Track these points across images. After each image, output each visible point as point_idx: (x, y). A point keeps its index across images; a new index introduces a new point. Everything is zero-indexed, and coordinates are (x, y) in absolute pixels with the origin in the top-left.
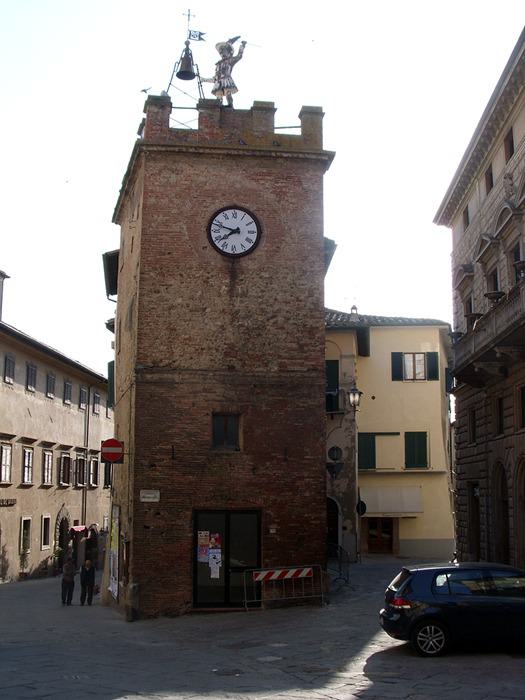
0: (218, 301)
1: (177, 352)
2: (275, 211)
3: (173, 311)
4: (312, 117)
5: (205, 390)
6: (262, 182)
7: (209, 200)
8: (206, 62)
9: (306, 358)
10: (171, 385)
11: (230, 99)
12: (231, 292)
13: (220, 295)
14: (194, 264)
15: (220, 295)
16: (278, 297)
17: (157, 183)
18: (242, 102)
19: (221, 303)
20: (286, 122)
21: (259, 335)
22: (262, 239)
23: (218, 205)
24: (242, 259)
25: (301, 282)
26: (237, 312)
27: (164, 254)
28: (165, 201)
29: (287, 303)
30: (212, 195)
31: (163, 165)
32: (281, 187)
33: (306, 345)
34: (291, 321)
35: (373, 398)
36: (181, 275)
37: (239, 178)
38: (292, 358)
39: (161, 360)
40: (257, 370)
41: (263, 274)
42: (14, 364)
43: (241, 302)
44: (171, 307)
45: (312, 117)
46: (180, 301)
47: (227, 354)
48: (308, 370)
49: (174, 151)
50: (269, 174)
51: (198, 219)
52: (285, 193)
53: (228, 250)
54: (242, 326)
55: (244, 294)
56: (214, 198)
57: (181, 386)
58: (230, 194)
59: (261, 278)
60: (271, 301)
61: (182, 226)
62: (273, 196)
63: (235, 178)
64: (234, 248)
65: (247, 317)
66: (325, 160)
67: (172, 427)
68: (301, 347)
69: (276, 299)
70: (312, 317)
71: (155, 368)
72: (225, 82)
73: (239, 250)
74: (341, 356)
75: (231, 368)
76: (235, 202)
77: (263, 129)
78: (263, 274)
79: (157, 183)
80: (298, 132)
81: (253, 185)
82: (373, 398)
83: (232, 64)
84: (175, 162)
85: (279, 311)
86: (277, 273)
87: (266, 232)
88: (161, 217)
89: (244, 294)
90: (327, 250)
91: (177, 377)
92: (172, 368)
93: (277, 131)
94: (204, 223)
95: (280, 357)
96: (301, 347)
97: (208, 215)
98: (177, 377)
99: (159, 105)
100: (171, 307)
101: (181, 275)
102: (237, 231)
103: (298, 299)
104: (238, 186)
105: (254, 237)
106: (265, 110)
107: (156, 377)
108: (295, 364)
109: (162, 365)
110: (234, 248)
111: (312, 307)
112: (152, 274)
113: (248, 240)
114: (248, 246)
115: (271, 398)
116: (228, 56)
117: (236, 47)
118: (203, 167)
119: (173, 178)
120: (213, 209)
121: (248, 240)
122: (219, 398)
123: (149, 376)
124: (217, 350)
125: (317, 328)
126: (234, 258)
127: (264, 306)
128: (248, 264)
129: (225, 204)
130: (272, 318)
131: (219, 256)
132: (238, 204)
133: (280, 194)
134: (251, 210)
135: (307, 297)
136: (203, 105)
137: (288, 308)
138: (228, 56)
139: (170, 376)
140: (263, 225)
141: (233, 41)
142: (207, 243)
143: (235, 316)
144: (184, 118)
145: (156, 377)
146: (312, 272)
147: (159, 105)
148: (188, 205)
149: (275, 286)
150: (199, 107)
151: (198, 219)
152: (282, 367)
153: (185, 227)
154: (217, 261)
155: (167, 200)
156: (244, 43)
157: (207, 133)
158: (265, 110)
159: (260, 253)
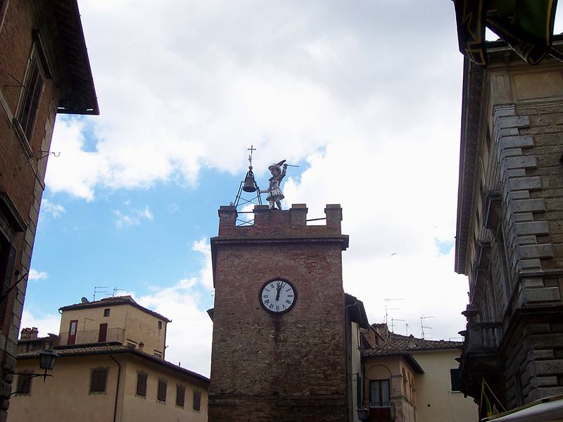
0: (266, 345)
1: (238, 382)
2: (307, 280)
3: (235, 354)
4: (334, 212)
5: (257, 410)
7: (261, 275)
8: (262, 176)
9: (331, 385)
10: (234, 407)
11: (279, 204)
12: (276, 339)
14: (251, 320)
18: (286, 205)
19: (269, 347)
20: (316, 216)
21: (296, 369)
23: (268, 278)
25: (327, 330)
26: (281, 353)
27: (229, 314)
29: (315, 345)
31: (230, 252)
33: (330, 375)
34: (319, 358)
35: (429, 406)
37: (281, 259)
38: (319, 385)
40: (295, 394)
42: (166, 386)
43: (283, 346)
44: (235, 351)
45: (334, 212)
47: (273, 383)
48: (332, 394)
49: (237, 244)
50: (302, 254)
53: (274, 310)
54: (284, 363)
55: (285, 341)
57: (240, 407)
59: (297, 328)
60: (304, 344)
63: (280, 259)
64: (277, 307)
65: (286, 356)
66: (343, 243)
68: (326, 376)
69: (308, 343)
70: (334, 354)
71: (223, 395)
72: (275, 192)
73: (282, 309)
74: (392, 377)
75: (275, 393)
77: (298, 223)
80: (324, 223)
82: (429, 406)
83: (280, 180)
84: (238, 250)
86: (309, 324)
89: (285, 341)
90: (361, 304)
91: (237, 401)
92: (234, 395)
93: (309, 223)
94: (256, 291)
95: (311, 384)
96: (326, 376)
97: (260, 286)
98: (237, 401)
99: (228, 213)
100: (235, 351)
102: (278, 297)
104: (281, 264)
105: (292, 300)
106: (301, 210)
107: (223, 401)
108: (322, 389)
110: (277, 307)
111: (334, 347)
112: (221, 329)
113: (287, 301)
114: (288, 306)
115: (305, 415)
116: (278, 172)
117: (282, 168)
118: (256, 253)
119: (236, 261)
120: (264, 281)
121: (287, 301)
122: (269, 416)
123: (218, 401)
124: (266, 381)
125: (338, 362)
126: (276, 316)
127: (299, 348)
128: (286, 318)
129: (272, 277)
130: (306, 356)
132: (281, 277)
133: (310, 268)
134: (290, 281)
135: (331, 341)
136: (257, 210)
137: (316, 349)
138: (278, 172)
139: (232, 400)
141: (281, 164)
143: (278, 356)
144: (247, 216)
145: (223, 401)
147: (228, 213)
148: (247, 280)
149: (307, 333)
150: (254, 211)
152: (313, 393)
153: (244, 294)
154: (266, 319)
156: (286, 165)
158: (301, 210)
159: (296, 310)
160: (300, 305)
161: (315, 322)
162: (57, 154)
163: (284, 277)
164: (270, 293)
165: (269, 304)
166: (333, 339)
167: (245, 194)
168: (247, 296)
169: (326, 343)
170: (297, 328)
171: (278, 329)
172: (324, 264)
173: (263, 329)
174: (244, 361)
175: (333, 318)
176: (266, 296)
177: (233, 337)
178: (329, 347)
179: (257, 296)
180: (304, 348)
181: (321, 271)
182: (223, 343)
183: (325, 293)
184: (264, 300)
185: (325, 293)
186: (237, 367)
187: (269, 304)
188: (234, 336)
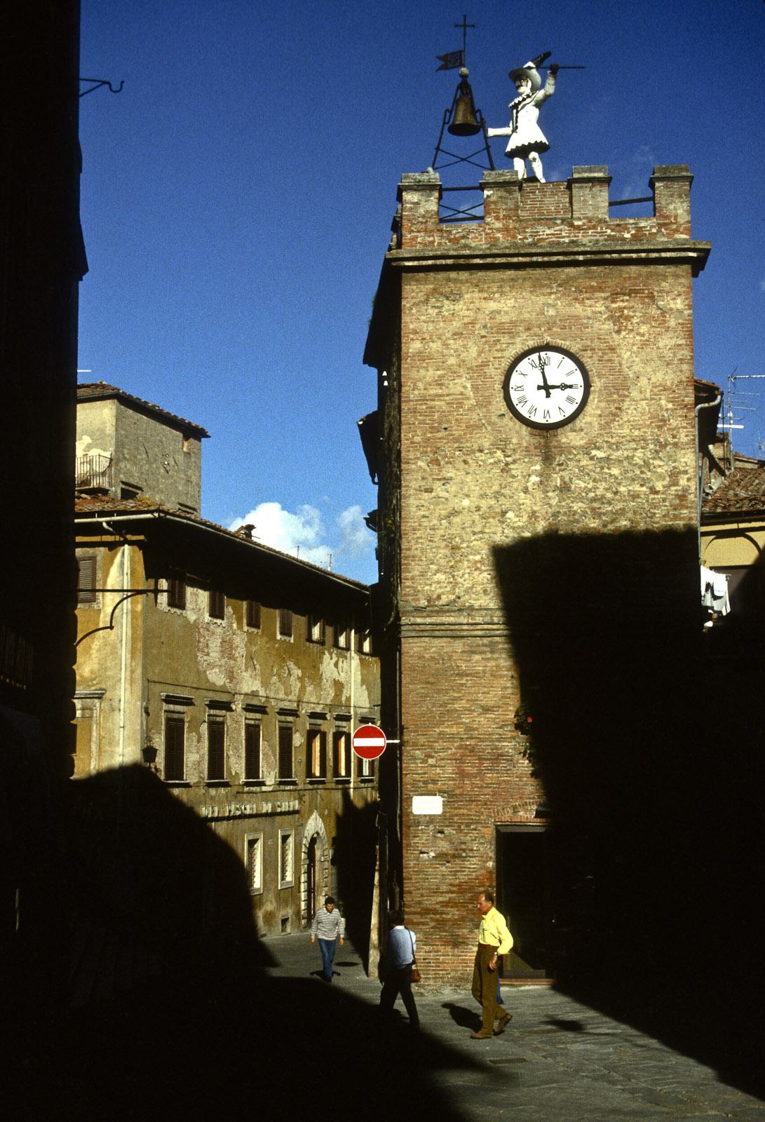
2: (612, 349)
3: (456, 520)
6: (588, 302)
7: (505, 339)
13: (526, 491)
15: (526, 491)
16: (622, 489)
17: (423, 318)
22: (591, 397)
23: (518, 348)
24: (559, 431)
28: (435, 346)
30: (509, 330)
32: (621, 309)
36: (465, 462)
39: (439, 597)
41: (594, 452)
44: (455, 513)
46: (466, 503)
50: (600, 289)
51: (491, 370)
52: (628, 318)
53: (538, 418)
56: (512, 334)
58: (539, 326)
59: (592, 458)
61: (462, 385)
62: (609, 326)
67: (460, 698)
69: (616, 493)
73: (556, 418)
76: (548, 339)
78: (594, 452)
79: (423, 318)
81: (578, 309)
85: (623, 510)
87: (597, 384)
88: (431, 372)
97: (505, 364)
100: (455, 513)
101: (465, 462)
103: (654, 491)
104: (552, 312)
109: (441, 603)
113: (570, 400)
127: (595, 505)
128: (568, 437)
129: (531, 344)
131: (525, 430)
135: (668, 487)
140: (593, 374)
142: (504, 408)
146: (675, 445)
148: (474, 351)
149: (615, 471)
151: (491, 370)
153: (469, 385)
155: (439, 343)
157: (498, 230)
159: (588, 419)
160: (597, 407)
161: (633, 445)
162: (114, 88)
163: (560, 342)
164: (526, 378)
165: (527, 406)
166: (676, 484)
167: (451, 142)
168: (475, 388)
169: (657, 492)
170: (592, 458)
171: (547, 459)
172: (654, 311)
173: (514, 462)
174: (474, 533)
175: (674, 437)
176: (519, 388)
177: (446, 481)
178: (664, 500)
179: (498, 386)
180: (609, 503)
181: (644, 329)
182: (426, 495)
183: (653, 380)
184: (514, 396)
185: (658, 377)
186: (459, 548)
187: (527, 406)
188: (451, 479)
